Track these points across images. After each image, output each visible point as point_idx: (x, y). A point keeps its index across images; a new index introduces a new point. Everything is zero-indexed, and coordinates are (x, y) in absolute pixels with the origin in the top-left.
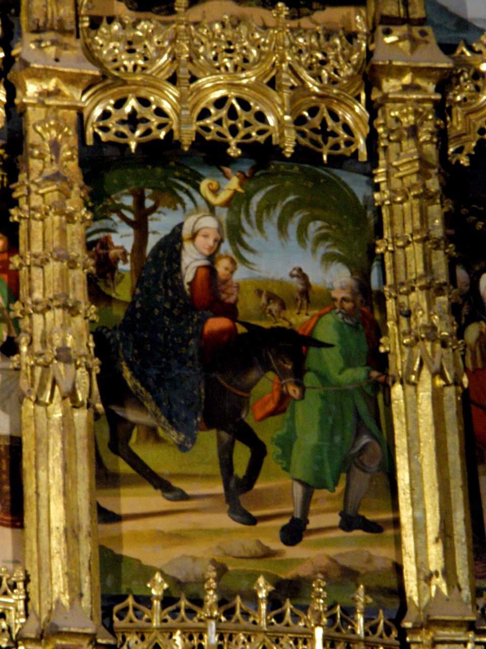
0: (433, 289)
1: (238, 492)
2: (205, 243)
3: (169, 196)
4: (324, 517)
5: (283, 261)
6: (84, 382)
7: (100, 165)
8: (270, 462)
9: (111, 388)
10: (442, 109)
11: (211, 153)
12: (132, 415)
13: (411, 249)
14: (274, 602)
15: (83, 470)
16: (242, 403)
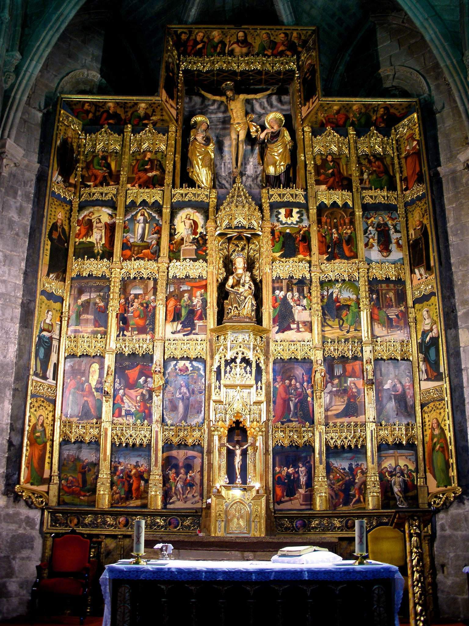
0: (366, 298)
1: (341, 327)
3: (331, 287)
5: (346, 295)
6: (320, 314)
7: (322, 283)
9: (324, 314)
10: (368, 273)
11: (337, 281)
14: (345, 342)
15: (320, 326)
16: (341, 315)
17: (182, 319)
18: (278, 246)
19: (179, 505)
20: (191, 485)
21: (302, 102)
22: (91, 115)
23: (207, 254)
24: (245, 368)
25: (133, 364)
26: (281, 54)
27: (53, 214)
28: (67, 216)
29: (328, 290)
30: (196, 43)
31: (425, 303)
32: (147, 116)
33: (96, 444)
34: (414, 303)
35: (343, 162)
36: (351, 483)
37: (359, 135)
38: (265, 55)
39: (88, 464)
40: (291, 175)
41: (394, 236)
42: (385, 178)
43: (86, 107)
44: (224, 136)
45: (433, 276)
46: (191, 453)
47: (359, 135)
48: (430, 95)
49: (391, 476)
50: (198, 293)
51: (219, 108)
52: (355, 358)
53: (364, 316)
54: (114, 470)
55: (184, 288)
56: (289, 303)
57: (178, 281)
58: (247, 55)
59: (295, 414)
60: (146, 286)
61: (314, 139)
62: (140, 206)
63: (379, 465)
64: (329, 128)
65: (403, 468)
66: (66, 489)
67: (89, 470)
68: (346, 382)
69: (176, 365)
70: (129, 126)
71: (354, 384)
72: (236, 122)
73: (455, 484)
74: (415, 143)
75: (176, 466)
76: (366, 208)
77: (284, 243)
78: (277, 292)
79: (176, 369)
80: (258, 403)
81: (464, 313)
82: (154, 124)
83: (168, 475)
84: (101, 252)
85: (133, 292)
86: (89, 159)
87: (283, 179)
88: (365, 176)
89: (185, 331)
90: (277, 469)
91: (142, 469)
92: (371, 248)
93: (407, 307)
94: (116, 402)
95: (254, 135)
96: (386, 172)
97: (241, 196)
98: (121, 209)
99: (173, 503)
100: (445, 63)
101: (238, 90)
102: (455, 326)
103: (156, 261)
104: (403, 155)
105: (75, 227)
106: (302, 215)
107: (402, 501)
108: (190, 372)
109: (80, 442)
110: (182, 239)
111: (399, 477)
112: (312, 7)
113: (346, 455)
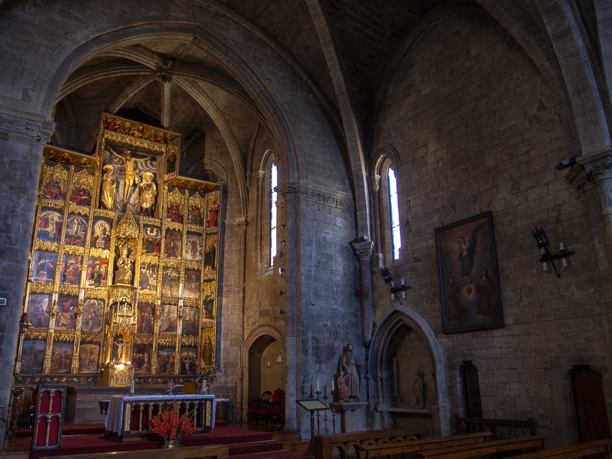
5: (174, 274)
6: (161, 282)
11: (171, 267)
13: (182, 273)
18: (145, 246)
19: (86, 371)
20: (93, 362)
21: (166, 172)
22: (52, 156)
23: (110, 246)
24: (129, 308)
25: (68, 299)
26: (159, 141)
30: (115, 124)
31: (209, 283)
32: (85, 164)
33: (45, 340)
34: (204, 282)
35: (181, 208)
36: (167, 363)
37: (190, 195)
38: (150, 140)
39: (39, 351)
40: (154, 208)
41: (199, 248)
42: (199, 219)
43: (52, 152)
44: (121, 179)
45: (215, 272)
46: (93, 346)
47: (190, 195)
48: (227, 182)
50: (104, 266)
51: (119, 161)
52: (175, 305)
53: (181, 285)
54: (53, 353)
55: (97, 262)
57: (94, 258)
58: (141, 138)
59: (144, 330)
60: (77, 260)
61: (169, 194)
62: (77, 215)
63: (181, 354)
64: (176, 189)
67: (39, 354)
70: (73, 166)
72: (129, 173)
73: (214, 365)
74: (216, 206)
76: (189, 233)
77: (148, 245)
78: (142, 270)
80: (134, 324)
81: (226, 290)
82: (87, 168)
86: (48, 181)
87: (149, 210)
88: (190, 217)
90: (135, 354)
91: (68, 353)
93: (200, 283)
95: (137, 182)
96: (200, 216)
97: (130, 219)
98: (66, 215)
99: (83, 370)
100: (238, 173)
101: (133, 155)
102: (222, 296)
103: (84, 247)
104: (209, 209)
105: (38, 221)
106: (158, 232)
109: (36, 339)
110: (98, 236)
112: (178, 118)
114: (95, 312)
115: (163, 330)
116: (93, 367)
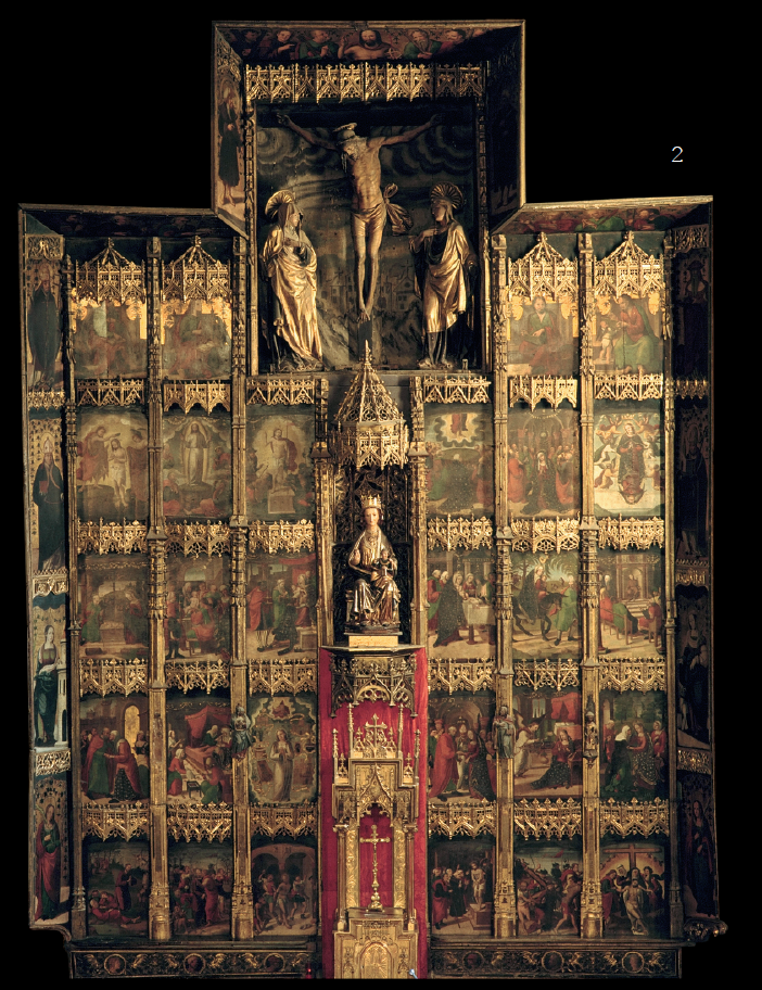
1: (545, 634)
2: (539, 573)
3: (531, 562)
4: (565, 639)
8: (552, 626)
12: (520, 617)
17: (276, 625)
27: (35, 444)
28: (60, 439)
29: (525, 567)
43: (71, 218)
46: (297, 849)
49: (623, 886)
54: (174, 881)
56: (456, 593)
59: (465, 783)
63: (603, 867)
65: (642, 872)
66: (99, 915)
68: (551, 729)
69: (266, 705)
71: (566, 732)
75: (274, 870)
78: (437, 572)
79: (268, 711)
83: (261, 884)
84: (125, 505)
85: (189, 578)
89: (281, 646)
91: (219, 876)
92: (607, 487)
94: (171, 769)
99: (271, 928)
107: (639, 926)
108: (291, 716)
110: (270, 477)
111: (636, 887)
113: (548, 850)
114: (288, 739)
115: (532, 784)
116: (303, 917)
